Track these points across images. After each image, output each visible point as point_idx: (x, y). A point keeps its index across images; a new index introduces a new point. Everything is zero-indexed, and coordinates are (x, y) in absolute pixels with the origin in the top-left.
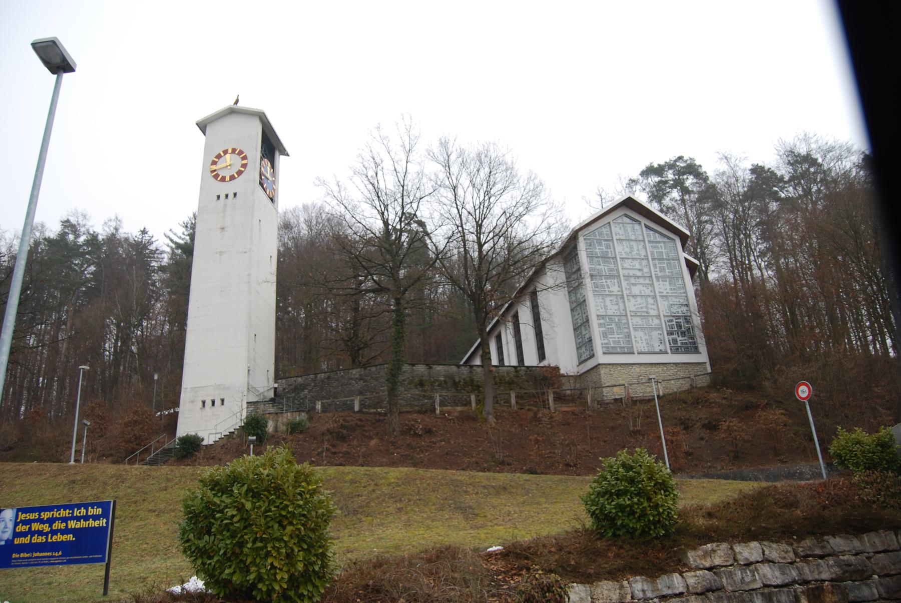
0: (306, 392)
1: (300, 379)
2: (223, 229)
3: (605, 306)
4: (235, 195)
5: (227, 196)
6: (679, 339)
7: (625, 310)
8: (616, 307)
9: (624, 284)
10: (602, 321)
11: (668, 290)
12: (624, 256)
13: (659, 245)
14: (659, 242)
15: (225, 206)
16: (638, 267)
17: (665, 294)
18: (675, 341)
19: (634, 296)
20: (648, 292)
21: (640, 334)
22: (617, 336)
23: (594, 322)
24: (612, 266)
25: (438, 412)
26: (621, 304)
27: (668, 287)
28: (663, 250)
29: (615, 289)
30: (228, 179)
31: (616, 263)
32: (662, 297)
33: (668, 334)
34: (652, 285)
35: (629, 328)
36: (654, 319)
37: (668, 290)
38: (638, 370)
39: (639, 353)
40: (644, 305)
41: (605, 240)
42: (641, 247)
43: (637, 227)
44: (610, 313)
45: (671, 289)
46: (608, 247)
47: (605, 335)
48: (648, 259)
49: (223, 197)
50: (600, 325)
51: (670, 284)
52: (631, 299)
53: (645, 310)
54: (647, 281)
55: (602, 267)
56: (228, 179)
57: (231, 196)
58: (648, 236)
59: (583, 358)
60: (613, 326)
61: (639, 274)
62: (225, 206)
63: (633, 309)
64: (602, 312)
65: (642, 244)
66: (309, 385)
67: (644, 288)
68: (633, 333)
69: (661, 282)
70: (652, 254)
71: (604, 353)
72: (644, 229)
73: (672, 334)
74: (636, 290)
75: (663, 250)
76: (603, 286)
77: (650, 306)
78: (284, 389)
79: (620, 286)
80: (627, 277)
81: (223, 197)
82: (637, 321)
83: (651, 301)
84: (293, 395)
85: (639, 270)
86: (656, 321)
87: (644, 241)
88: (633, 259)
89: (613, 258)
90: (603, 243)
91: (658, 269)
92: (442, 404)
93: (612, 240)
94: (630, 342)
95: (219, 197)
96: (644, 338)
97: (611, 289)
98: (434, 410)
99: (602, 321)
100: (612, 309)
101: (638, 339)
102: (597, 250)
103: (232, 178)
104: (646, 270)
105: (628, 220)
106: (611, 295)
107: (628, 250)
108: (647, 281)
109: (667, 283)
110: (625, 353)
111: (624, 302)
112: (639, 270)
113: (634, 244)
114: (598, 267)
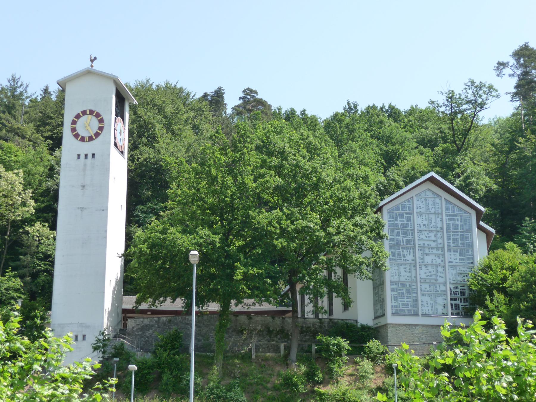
0: (151, 331)
1: (146, 320)
2: (83, 186)
3: (399, 274)
4: (93, 155)
5: (86, 156)
6: (461, 304)
7: (416, 277)
8: (409, 274)
9: (418, 254)
10: (395, 286)
11: (458, 260)
12: (422, 228)
13: (456, 218)
14: (456, 216)
15: (85, 165)
16: (433, 238)
17: (454, 264)
18: (457, 306)
19: (427, 266)
20: (439, 261)
21: (426, 299)
22: (406, 300)
23: (388, 287)
24: (410, 237)
25: (254, 357)
26: (413, 272)
27: (458, 257)
28: (459, 223)
29: (410, 258)
30: (87, 139)
31: (413, 234)
32: (451, 266)
33: (451, 299)
34: (444, 255)
35: (417, 293)
36: (441, 286)
37: (458, 260)
38: (420, 330)
39: (423, 315)
40: (434, 273)
41: (407, 214)
42: (438, 219)
43: (438, 200)
44: (402, 279)
45: (461, 259)
46: (409, 219)
47: (396, 299)
48: (443, 232)
49: (82, 156)
50: (393, 290)
51: (460, 254)
52: (424, 268)
53: (434, 277)
54: (440, 252)
55: (401, 238)
56: (87, 139)
57: (90, 156)
58: (447, 209)
59: (378, 314)
60: (404, 291)
61: (433, 244)
62: (85, 165)
63: (424, 276)
64: (395, 279)
65: (440, 216)
66: (153, 326)
67: (436, 258)
68: (420, 298)
69: (452, 253)
70: (448, 226)
71: (393, 314)
72: (444, 202)
73: (455, 299)
74: (428, 259)
75: (459, 223)
76: (399, 255)
77: (439, 274)
78: (133, 328)
79: (414, 256)
80: (422, 248)
81: (82, 156)
82: (426, 286)
83: (440, 269)
84: (140, 333)
85: (434, 241)
86: (443, 288)
87: (442, 214)
88: (430, 231)
89: (411, 230)
90: (405, 215)
91: (451, 241)
92: (257, 351)
93: (413, 213)
94: (416, 306)
95: (79, 156)
96: (430, 302)
97: (407, 258)
98: (250, 357)
99: (395, 286)
100: (405, 276)
101: (425, 303)
102: (399, 223)
103: (91, 139)
104: (440, 241)
105: (429, 194)
106: (405, 264)
107: (426, 222)
108: (440, 252)
109: (458, 254)
110: (399, 325)
111: (416, 270)
112: (434, 241)
113: (433, 217)
114: (397, 238)
